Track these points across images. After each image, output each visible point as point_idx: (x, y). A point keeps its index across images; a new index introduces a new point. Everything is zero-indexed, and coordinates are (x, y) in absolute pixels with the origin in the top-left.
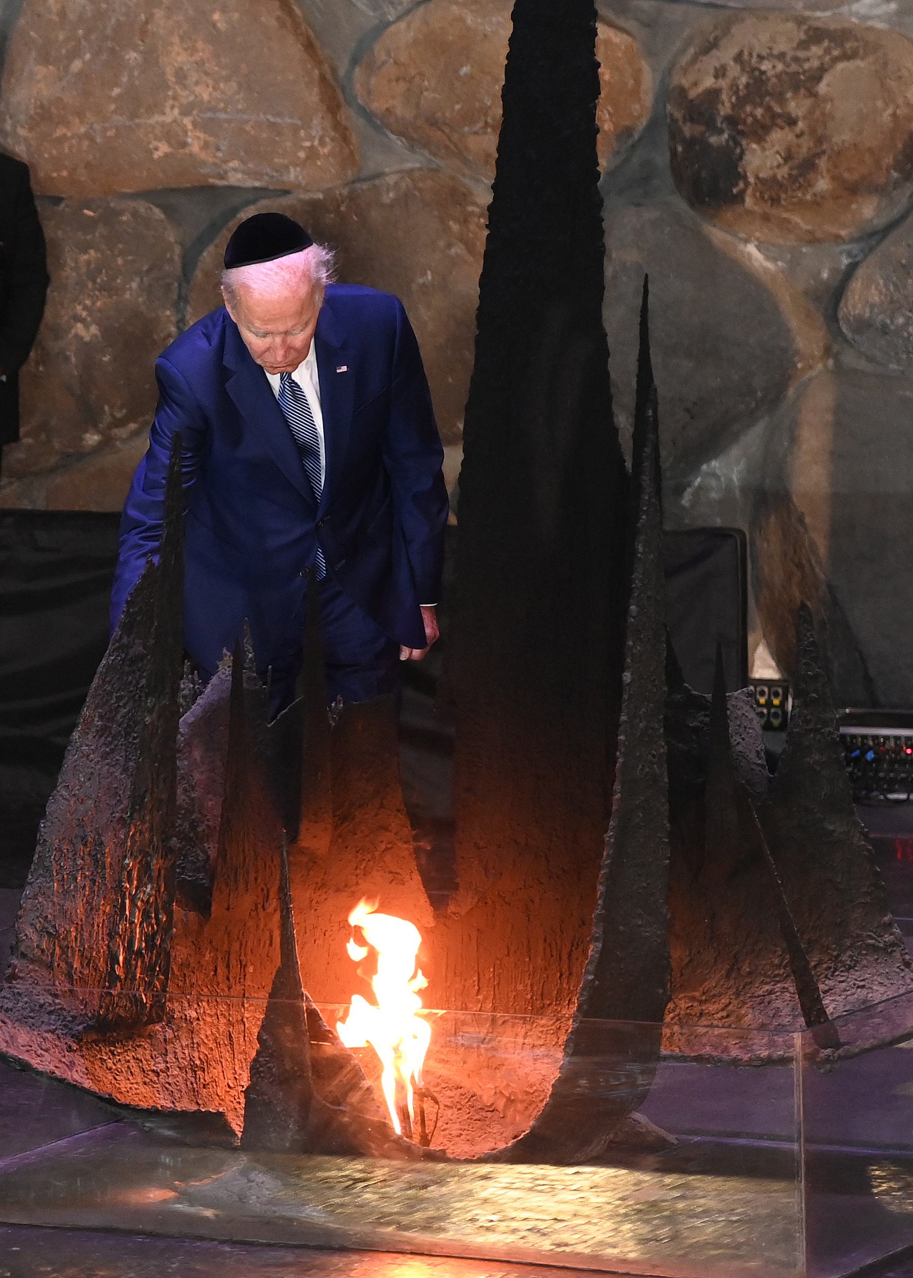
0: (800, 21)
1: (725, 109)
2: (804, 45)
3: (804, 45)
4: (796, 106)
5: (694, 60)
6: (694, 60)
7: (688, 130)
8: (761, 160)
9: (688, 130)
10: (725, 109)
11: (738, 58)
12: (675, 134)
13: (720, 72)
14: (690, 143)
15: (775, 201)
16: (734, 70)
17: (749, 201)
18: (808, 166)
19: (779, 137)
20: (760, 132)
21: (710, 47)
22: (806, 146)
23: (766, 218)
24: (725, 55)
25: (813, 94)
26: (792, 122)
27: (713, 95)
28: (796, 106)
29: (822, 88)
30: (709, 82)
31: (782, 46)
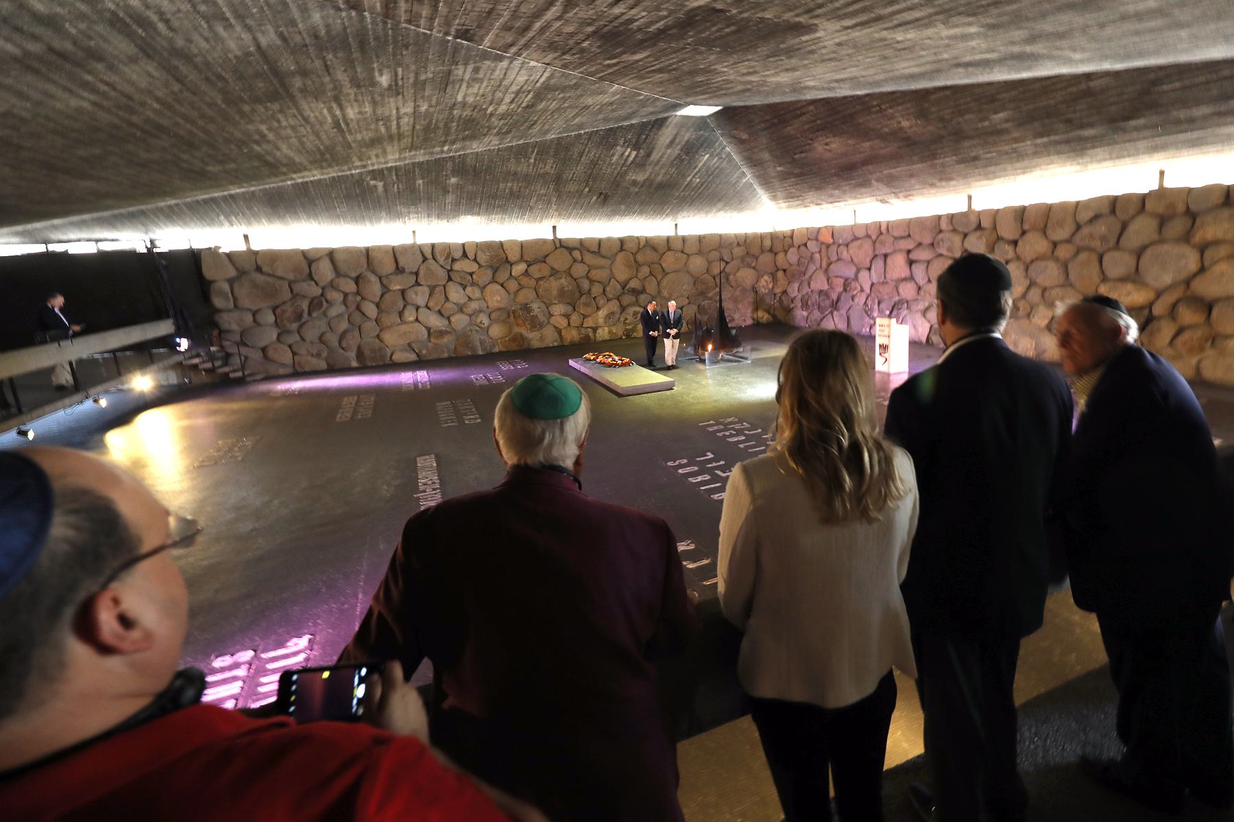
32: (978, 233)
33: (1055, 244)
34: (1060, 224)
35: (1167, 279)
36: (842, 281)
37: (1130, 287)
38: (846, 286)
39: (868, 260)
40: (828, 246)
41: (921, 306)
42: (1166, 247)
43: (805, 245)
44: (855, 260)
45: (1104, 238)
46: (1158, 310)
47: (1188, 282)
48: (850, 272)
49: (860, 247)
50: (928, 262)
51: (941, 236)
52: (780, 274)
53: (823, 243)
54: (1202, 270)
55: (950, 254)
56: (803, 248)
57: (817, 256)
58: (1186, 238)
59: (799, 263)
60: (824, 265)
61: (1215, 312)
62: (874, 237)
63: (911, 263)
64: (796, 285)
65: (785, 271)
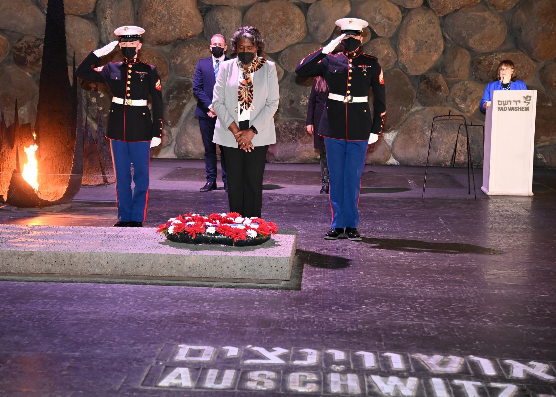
0: (35, 37)
1: (23, 50)
2: (36, 41)
3: (36, 41)
4: (36, 50)
5: (18, 42)
6: (18, 42)
7: (17, 53)
9: (17, 53)
10: (23, 50)
11: (25, 42)
12: (14, 54)
13: (22, 44)
14: (18, 55)
15: (33, 65)
16: (25, 44)
17: (28, 65)
19: (33, 55)
20: (30, 54)
21: (20, 40)
22: (38, 56)
23: (31, 68)
24: (23, 41)
25: (38, 48)
26: (35, 53)
27: (21, 48)
28: (36, 50)
29: (40, 47)
30: (21, 46)
31: (32, 41)
50: (245, 10)
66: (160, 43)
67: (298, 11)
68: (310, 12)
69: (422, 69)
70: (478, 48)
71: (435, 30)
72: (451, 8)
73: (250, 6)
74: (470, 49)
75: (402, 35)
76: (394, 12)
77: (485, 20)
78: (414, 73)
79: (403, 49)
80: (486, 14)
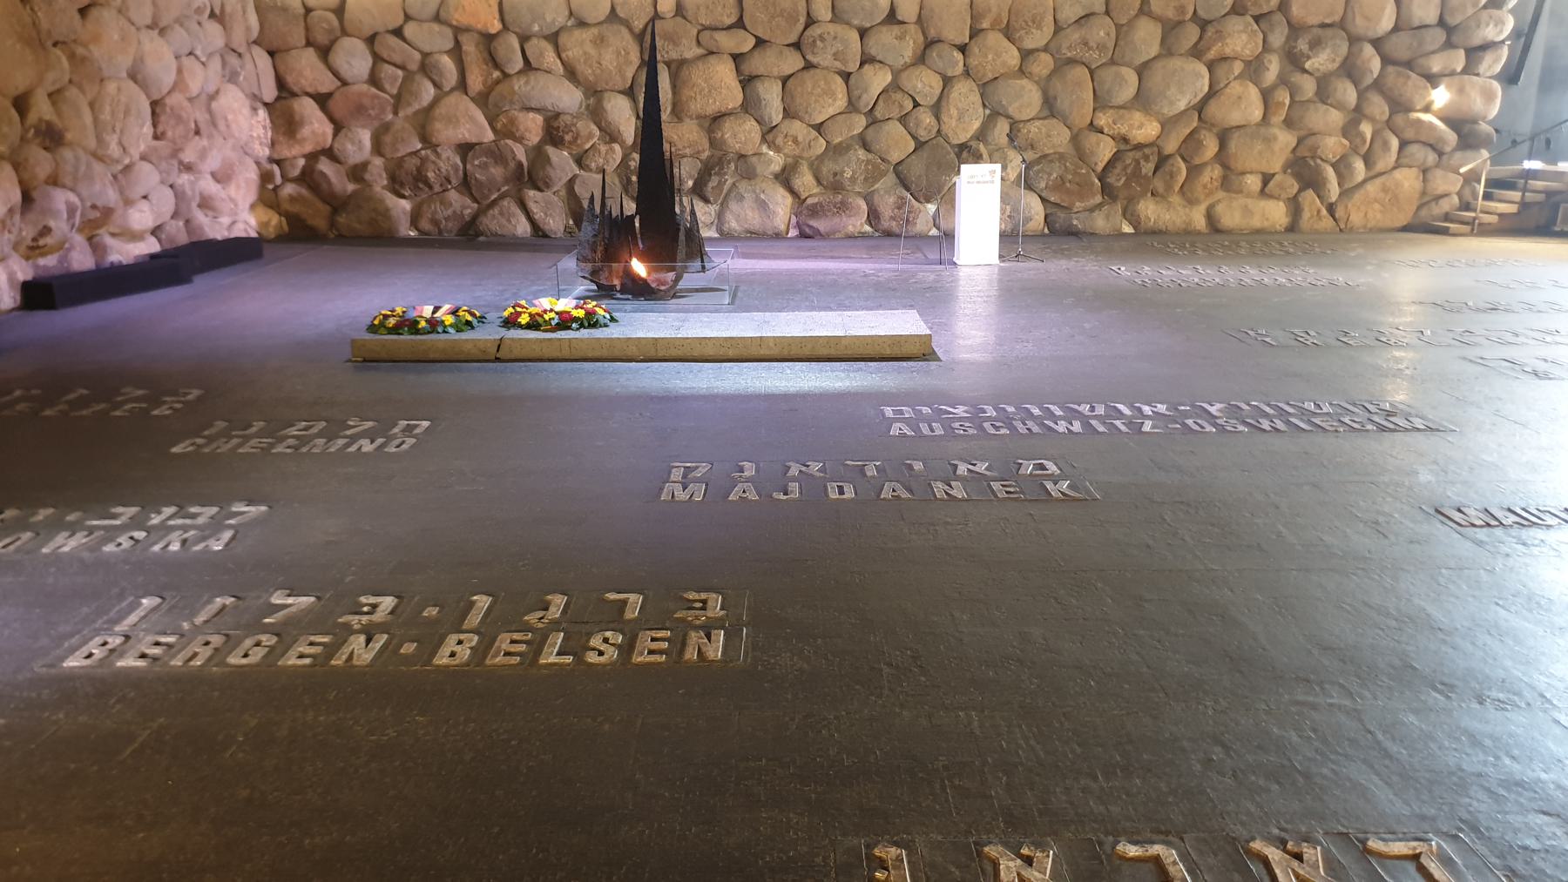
8: (568, 138)
18: (575, 139)
32: (896, 30)
33: (1026, 54)
34: (1037, 22)
35: (1182, 105)
36: (539, 119)
37: (1138, 116)
38: (554, 133)
39: (630, 75)
40: (488, 39)
41: (776, 161)
42: (1176, 63)
43: (398, 32)
44: (586, 71)
45: (1101, 47)
46: (1171, 146)
47: (1200, 107)
48: (568, 98)
49: (600, 41)
50: (785, 81)
51: (815, 31)
52: (307, 108)
53: (458, 31)
54: (1213, 93)
55: (838, 64)
56: (393, 41)
57: (447, 63)
58: (1196, 52)
59: (374, 80)
60: (476, 82)
61: (1233, 145)
62: (638, 25)
63: (747, 81)
64: (366, 137)
65: (322, 100)
66: (699, 117)
67: (839, 80)
68: (852, 80)
69: (963, 137)
70: (1017, 117)
71: (976, 98)
72: (990, 76)
73: (790, 76)
74: (1008, 117)
75: (944, 103)
76: (937, 83)
77: (1023, 88)
78: (956, 142)
79: (944, 118)
80: (1025, 82)
